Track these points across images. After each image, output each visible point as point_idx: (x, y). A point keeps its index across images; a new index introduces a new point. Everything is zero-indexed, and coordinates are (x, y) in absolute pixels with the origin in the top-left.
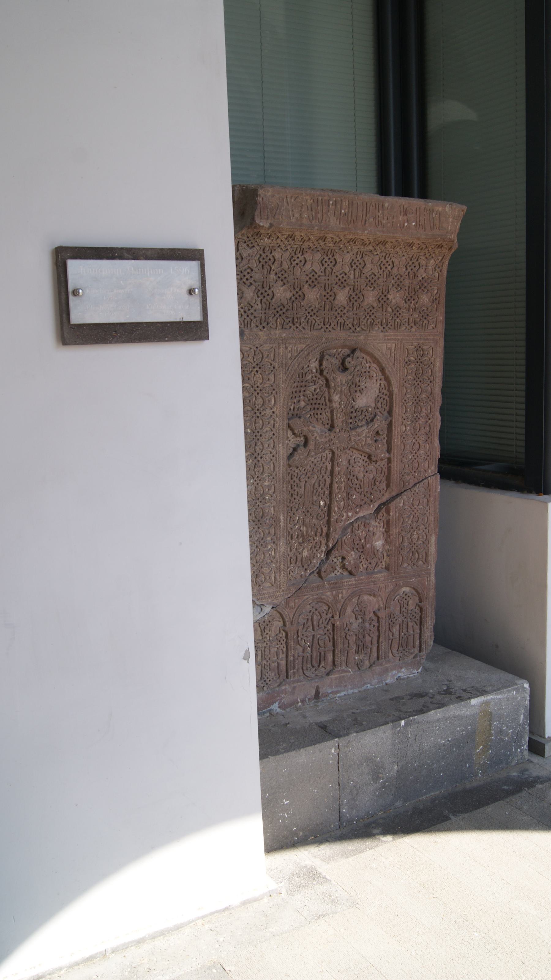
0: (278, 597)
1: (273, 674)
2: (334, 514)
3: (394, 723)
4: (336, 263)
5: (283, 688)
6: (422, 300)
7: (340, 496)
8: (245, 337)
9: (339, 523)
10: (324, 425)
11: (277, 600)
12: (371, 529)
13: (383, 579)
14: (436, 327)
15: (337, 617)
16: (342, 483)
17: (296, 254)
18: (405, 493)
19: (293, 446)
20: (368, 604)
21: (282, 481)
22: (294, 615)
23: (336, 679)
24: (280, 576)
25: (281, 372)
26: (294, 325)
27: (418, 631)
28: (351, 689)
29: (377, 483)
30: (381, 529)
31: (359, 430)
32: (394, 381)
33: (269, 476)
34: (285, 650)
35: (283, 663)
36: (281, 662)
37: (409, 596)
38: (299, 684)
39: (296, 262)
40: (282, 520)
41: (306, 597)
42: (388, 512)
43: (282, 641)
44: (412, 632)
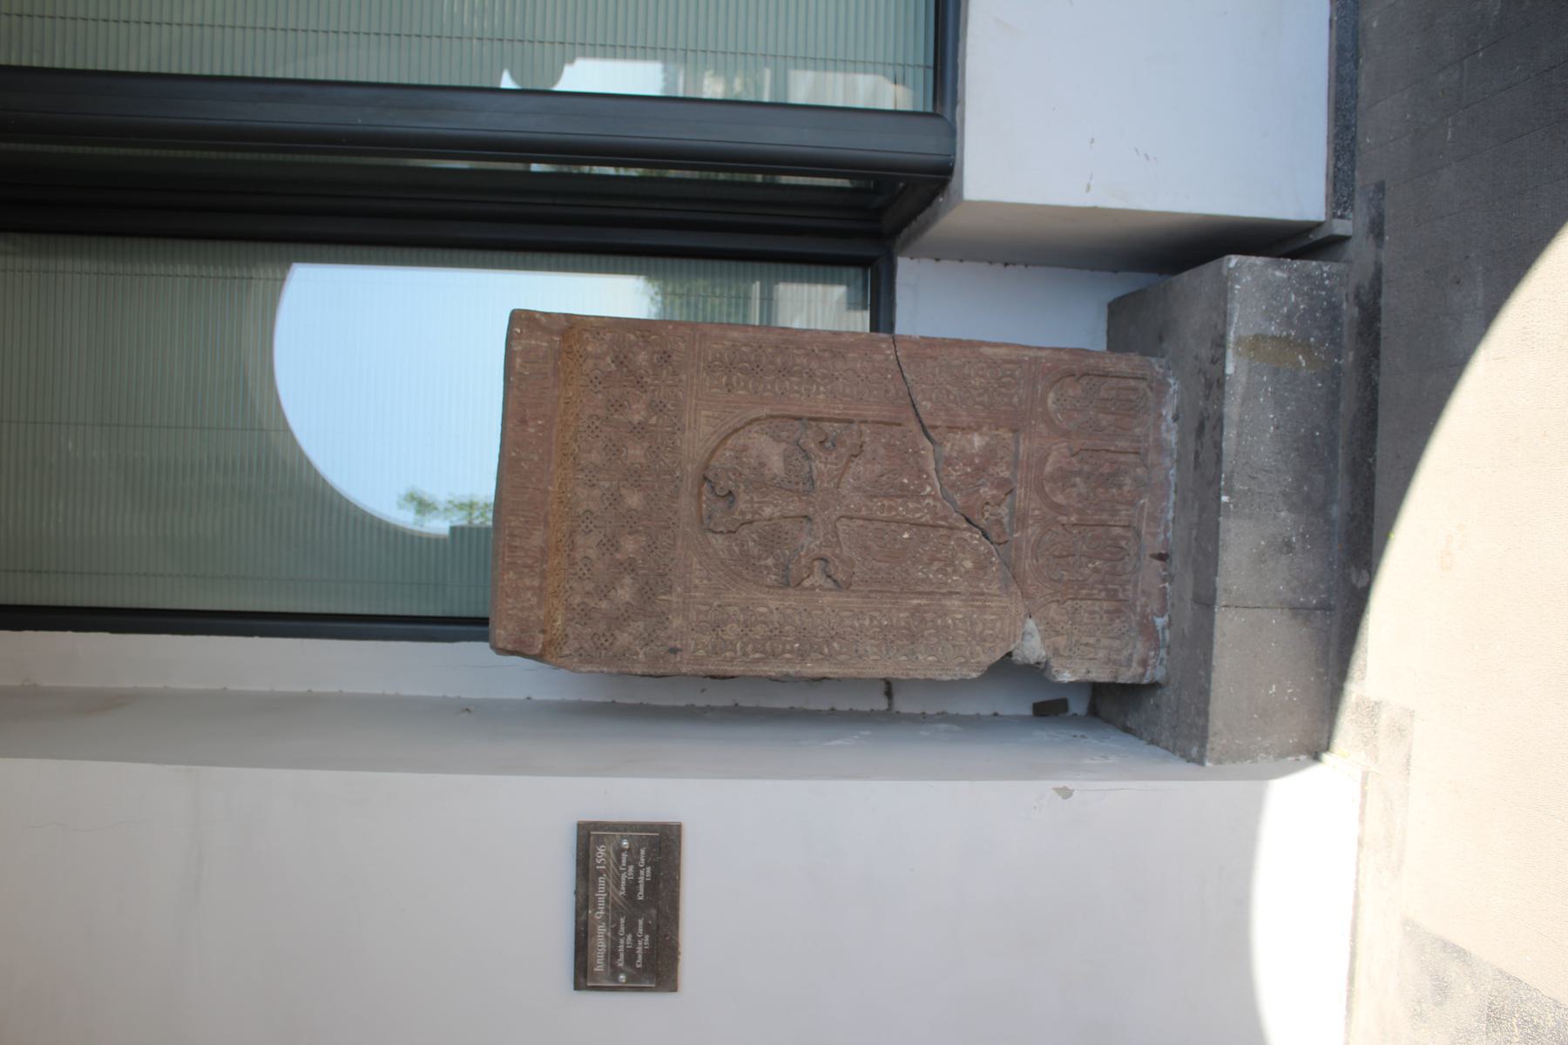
1: (1118, 621)
2: (924, 520)
3: (1222, 513)
4: (589, 511)
5: (1138, 609)
6: (644, 363)
7: (901, 509)
8: (679, 646)
10: (802, 528)
12: (954, 454)
13: (1027, 441)
14: (682, 337)
15: (1064, 519)
16: (883, 505)
17: (576, 574)
18: (913, 397)
19: (824, 577)
20: (1059, 465)
22: (1046, 587)
26: (666, 574)
27: (1115, 380)
30: (958, 436)
32: (753, 414)
33: (859, 619)
34: (1089, 602)
35: (1105, 605)
36: (1105, 608)
37: (1062, 395)
38: (1140, 584)
39: (586, 572)
40: (919, 601)
41: (1027, 567)
42: (935, 427)
43: (1077, 606)
44: (1114, 392)
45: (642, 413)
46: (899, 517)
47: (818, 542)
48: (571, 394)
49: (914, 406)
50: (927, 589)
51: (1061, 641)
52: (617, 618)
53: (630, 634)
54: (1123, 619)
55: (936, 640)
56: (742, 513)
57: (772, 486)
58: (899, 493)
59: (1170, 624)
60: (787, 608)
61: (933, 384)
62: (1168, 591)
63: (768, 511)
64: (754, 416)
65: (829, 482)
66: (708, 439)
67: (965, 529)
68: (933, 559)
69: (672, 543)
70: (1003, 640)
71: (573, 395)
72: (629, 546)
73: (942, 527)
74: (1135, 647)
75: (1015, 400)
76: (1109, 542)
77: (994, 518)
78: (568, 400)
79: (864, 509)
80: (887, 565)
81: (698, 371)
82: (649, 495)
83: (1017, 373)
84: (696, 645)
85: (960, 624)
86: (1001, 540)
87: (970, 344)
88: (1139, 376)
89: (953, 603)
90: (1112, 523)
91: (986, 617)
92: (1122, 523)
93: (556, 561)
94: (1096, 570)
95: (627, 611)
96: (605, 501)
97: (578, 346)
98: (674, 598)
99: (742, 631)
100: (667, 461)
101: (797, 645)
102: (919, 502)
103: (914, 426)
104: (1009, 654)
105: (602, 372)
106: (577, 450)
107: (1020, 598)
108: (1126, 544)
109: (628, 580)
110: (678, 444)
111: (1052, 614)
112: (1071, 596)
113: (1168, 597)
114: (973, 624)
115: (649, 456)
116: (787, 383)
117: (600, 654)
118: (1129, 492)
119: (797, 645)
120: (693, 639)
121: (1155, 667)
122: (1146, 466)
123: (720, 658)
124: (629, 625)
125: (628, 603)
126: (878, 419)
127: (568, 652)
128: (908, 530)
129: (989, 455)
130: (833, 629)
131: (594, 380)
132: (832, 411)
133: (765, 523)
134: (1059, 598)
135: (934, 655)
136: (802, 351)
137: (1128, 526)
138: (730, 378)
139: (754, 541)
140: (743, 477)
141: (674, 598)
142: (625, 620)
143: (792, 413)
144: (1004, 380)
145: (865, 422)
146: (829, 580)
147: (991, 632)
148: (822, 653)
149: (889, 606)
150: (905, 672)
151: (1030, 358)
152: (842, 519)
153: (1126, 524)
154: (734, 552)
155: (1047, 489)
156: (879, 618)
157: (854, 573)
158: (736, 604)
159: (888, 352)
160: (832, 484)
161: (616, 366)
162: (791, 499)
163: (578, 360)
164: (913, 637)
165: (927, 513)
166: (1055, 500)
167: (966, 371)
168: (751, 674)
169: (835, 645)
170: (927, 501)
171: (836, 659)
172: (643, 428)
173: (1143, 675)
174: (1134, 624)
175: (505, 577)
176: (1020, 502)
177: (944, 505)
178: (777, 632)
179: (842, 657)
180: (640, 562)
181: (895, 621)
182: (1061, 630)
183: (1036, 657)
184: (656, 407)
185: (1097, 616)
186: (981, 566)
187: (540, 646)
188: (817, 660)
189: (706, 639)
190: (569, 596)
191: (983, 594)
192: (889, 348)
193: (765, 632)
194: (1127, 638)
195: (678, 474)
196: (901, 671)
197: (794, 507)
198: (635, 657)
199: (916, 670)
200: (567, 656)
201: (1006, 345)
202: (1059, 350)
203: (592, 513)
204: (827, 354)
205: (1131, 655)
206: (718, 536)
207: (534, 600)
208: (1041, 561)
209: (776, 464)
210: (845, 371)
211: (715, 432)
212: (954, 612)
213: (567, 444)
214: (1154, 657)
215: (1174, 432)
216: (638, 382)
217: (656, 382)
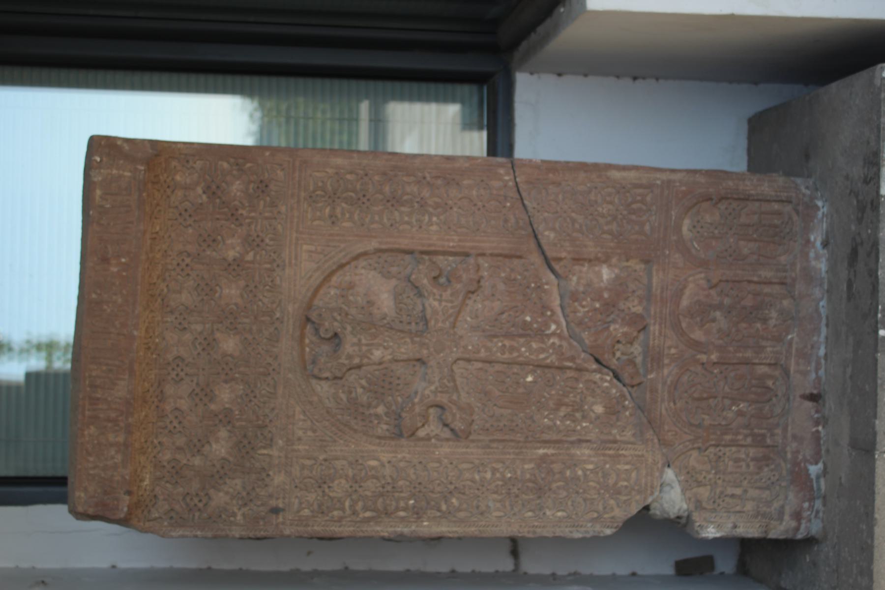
0: (654, 460)
1: (766, 469)
2: (548, 361)
3: (880, 348)
4: (179, 357)
5: (789, 456)
6: (238, 194)
7: (523, 349)
8: (281, 505)
9: (564, 350)
10: (415, 372)
11: (658, 462)
12: (581, 289)
14: (281, 165)
15: (703, 358)
16: (504, 346)
17: (166, 427)
18: (535, 226)
19: (441, 426)
21: (488, 450)
22: (686, 433)
23: (797, 364)
24: (625, 456)
25: (332, 448)
26: (266, 426)
27: (757, 204)
28: (819, 336)
29: (513, 276)
30: (585, 269)
31: (429, 312)
32: (360, 248)
33: (479, 471)
34: (734, 449)
35: (752, 452)
36: (751, 455)
37: (698, 222)
38: (790, 428)
39: (177, 426)
41: (664, 412)
42: (560, 259)
43: (720, 454)
44: (756, 217)
45: (238, 248)
46: (521, 359)
47: (433, 388)
48: (158, 228)
49: (536, 236)
50: (555, 437)
51: (704, 493)
52: (212, 476)
53: (227, 493)
54: (773, 467)
55: (565, 494)
56: (350, 357)
57: (382, 326)
58: (521, 331)
59: (825, 472)
60: (401, 461)
61: (557, 212)
62: (822, 435)
63: (377, 354)
64: (361, 250)
65: (444, 322)
66: (311, 277)
67: (595, 371)
68: (559, 404)
69: (272, 391)
70: (639, 492)
71: (161, 229)
72: (225, 395)
73: (569, 368)
74: (786, 498)
75: (647, 227)
76: (754, 382)
77: (625, 357)
78: (154, 236)
79: (483, 350)
80: (510, 411)
81: (298, 202)
82: (246, 338)
83: (648, 198)
84: (301, 503)
85: (592, 475)
86: (635, 382)
87: (596, 168)
88: (784, 198)
89: (583, 452)
90: (757, 361)
91: (619, 466)
92: (768, 361)
93: (144, 413)
94: (740, 413)
95: (223, 467)
96: (198, 346)
97: (165, 175)
98: (274, 452)
99: (351, 487)
100: (266, 300)
101: (412, 502)
102: (543, 342)
103: (536, 259)
104: (647, 508)
105: (193, 205)
106: (165, 290)
107: (657, 446)
108: (773, 384)
109: (223, 433)
110: (278, 280)
111: (692, 462)
112: (713, 443)
113: (822, 442)
114: (606, 475)
115: (245, 296)
116: (396, 214)
117: (194, 515)
118: (775, 326)
119: (412, 502)
120: (297, 497)
121: (810, 521)
122: (793, 297)
123: (327, 518)
124: (225, 483)
125: (223, 459)
126: (496, 252)
127: (157, 515)
128: (533, 372)
129: (619, 288)
130: (451, 483)
131: (183, 213)
132: (446, 244)
133: (375, 367)
134: (700, 445)
135: (563, 511)
136: (412, 179)
137: (775, 364)
138: (334, 208)
139: (363, 387)
140: (350, 317)
141: (274, 452)
142: (221, 478)
143: (403, 247)
144: (635, 206)
145: (483, 255)
146: (446, 429)
147: (625, 483)
148: (439, 510)
149: (512, 456)
150: (531, 529)
151: (663, 182)
152: (458, 362)
153: (773, 362)
154: (341, 400)
155: (684, 325)
156: (501, 470)
157: (473, 421)
158: (344, 458)
159: (507, 178)
160: (447, 323)
161: (208, 197)
162: (403, 341)
163: (165, 191)
164: (540, 491)
165: (552, 354)
166: (692, 336)
167: (592, 197)
168: (361, 534)
169: (454, 501)
170: (551, 341)
171: (455, 516)
172: (238, 265)
173: (797, 529)
174: (784, 473)
175: (86, 433)
176: (654, 340)
177: (570, 344)
178: (389, 488)
179: (462, 515)
180: (237, 413)
181: (519, 473)
182: (704, 480)
183: (676, 511)
184: (252, 242)
185: (743, 464)
186: (613, 411)
187: (126, 509)
188: (435, 517)
189: (311, 497)
190: (159, 452)
191: (615, 442)
192: (507, 174)
193: (377, 487)
194: (778, 488)
195: (278, 315)
196: (526, 530)
197: (406, 349)
198: (232, 519)
199: (544, 527)
200: (155, 519)
201: (636, 168)
202: (695, 172)
203: (183, 360)
204: (439, 182)
205: (783, 507)
206: (323, 383)
207: (119, 458)
208: (679, 405)
209: (385, 302)
210: (460, 199)
211: (318, 269)
212: (585, 462)
213: (155, 284)
214: (808, 509)
215: (824, 260)
216: (232, 215)
217: (253, 214)
